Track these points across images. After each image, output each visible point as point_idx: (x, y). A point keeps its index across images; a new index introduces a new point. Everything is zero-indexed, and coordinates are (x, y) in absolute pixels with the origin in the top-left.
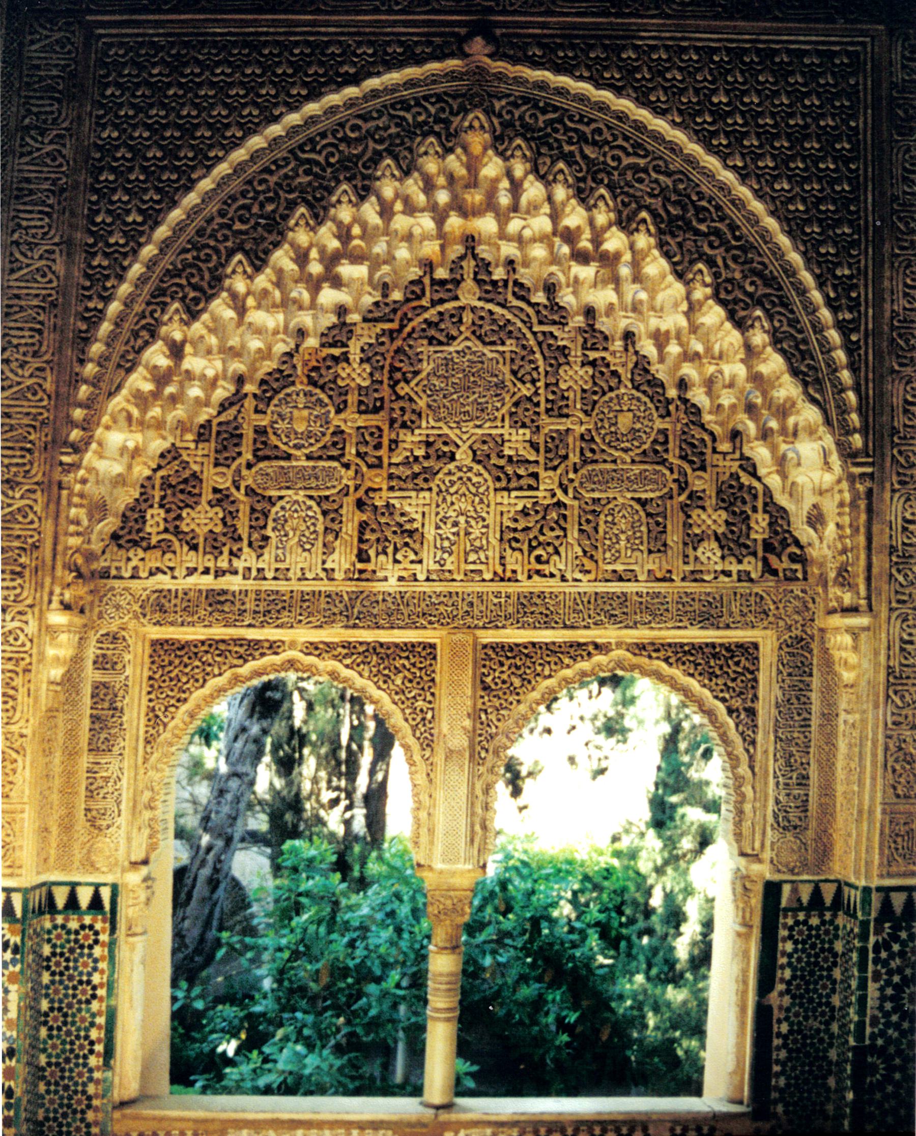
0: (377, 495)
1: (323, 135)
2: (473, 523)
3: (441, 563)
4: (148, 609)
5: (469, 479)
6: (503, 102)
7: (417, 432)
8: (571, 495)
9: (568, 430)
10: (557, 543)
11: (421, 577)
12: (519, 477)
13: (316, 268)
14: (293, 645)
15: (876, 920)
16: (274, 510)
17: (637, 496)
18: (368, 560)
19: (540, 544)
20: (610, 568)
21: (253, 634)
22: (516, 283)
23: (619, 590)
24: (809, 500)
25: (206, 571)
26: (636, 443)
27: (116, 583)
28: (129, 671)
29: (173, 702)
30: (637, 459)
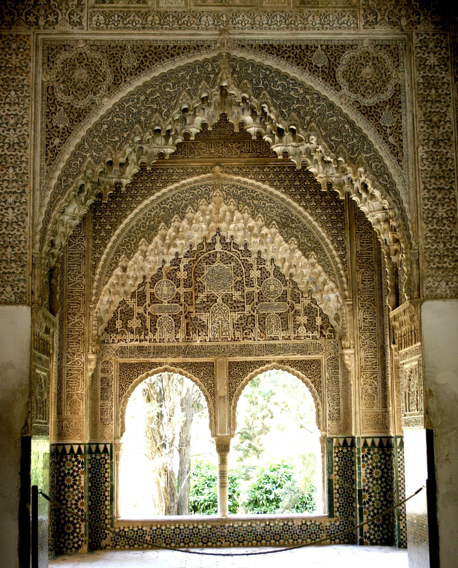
0: (192, 314)
1: (168, 199)
4: (118, 353)
11: (208, 340)
12: (238, 307)
13: (167, 241)
14: (166, 363)
16: (158, 320)
21: (153, 360)
24: (334, 312)
25: (137, 340)
27: (107, 345)
28: (113, 373)
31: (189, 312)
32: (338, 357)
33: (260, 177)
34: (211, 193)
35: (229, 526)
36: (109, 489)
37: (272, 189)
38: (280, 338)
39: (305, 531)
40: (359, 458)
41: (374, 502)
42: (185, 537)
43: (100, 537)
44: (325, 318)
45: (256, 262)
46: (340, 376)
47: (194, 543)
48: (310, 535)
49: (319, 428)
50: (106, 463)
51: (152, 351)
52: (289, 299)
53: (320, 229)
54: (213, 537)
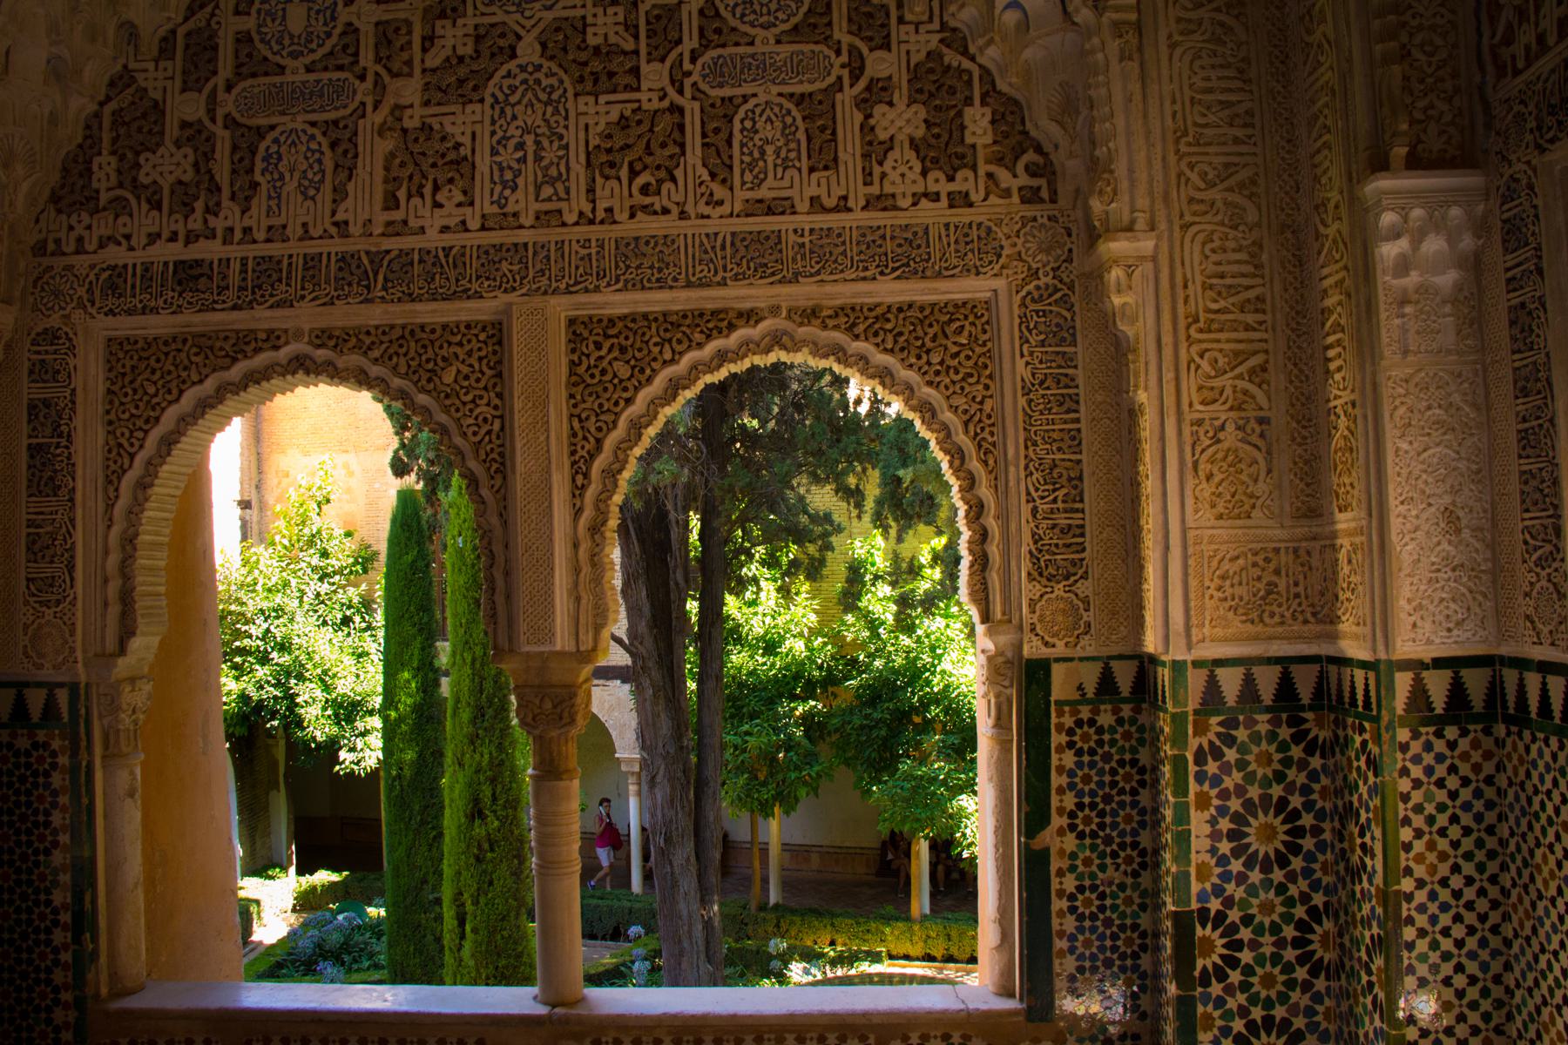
2: (546, 143)
3: (501, 203)
4: (97, 293)
5: (538, 82)
11: (474, 224)
12: (611, 75)
14: (298, 334)
15: (1196, 712)
17: (787, 89)
18: (398, 207)
19: (645, 167)
21: (240, 320)
23: (768, 228)
25: (173, 238)
26: (780, 15)
29: (139, 423)
30: (784, 38)
31: (397, 107)
32: (1071, 287)
36: (65, 878)
38: (802, 206)
40: (1179, 763)
41: (1248, 971)
44: (1008, 114)
46: (1080, 375)
49: (985, 618)
51: (234, 278)
52: (841, 34)
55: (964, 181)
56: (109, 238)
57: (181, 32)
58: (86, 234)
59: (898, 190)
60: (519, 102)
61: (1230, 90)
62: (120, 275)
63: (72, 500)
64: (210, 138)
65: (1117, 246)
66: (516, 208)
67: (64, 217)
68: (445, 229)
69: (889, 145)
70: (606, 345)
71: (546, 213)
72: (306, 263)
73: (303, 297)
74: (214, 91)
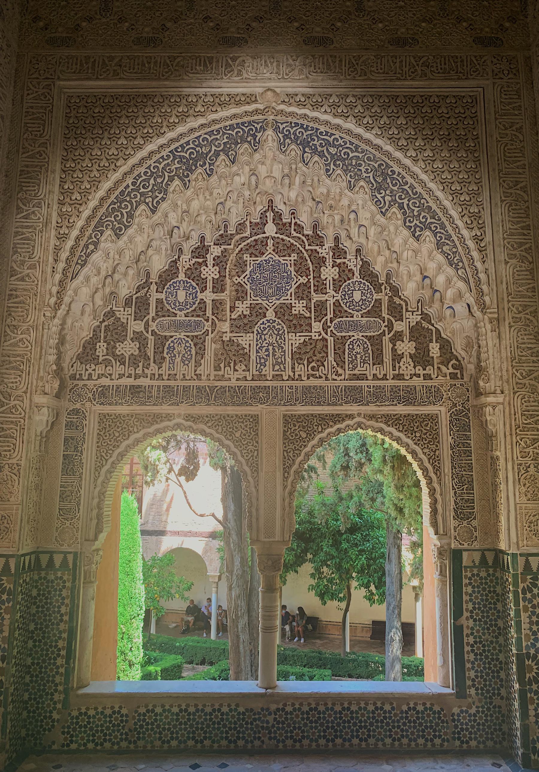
1: (188, 143)
4: (97, 396)
5: (274, 326)
6: (284, 125)
7: (245, 302)
8: (329, 334)
9: (327, 300)
10: (323, 360)
19: (313, 361)
20: (351, 372)
21: (156, 409)
22: (296, 224)
23: (358, 385)
25: (130, 376)
27: (81, 383)
29: (110, 447)
32: (469, 410)
33: (340, 111)
34: (259, 135)
35: (278, 710)
36: (65, 635)
37: (360, 131)
39: (415, 722)
42: (197, 728)
43: (41, 726)
45: (331, 254)
47: (213, 742)
48: (423, 731)
49: (436, 533)
50: (64, 587)
51: (154, 393)
52: (385, 314)
53: (440, 194)
54: (247, 729)
55: (429, 370)
56: (102, 375)
57: (134, 297)
58: (93, 373)
59: (405, 373)
60: (267, 334)
61: (531, 343)
62: (106, 390)
63: (80, 477)
64: (146, 338)
65: (491, 399)
66: (265, 373)
67: (84, 366)
68: (238, 379)
69: (402, 356)
70: (298, 425)
71: (277, 375)
72: (184, 389)
73: (182, 402)
74: (148, 321)
